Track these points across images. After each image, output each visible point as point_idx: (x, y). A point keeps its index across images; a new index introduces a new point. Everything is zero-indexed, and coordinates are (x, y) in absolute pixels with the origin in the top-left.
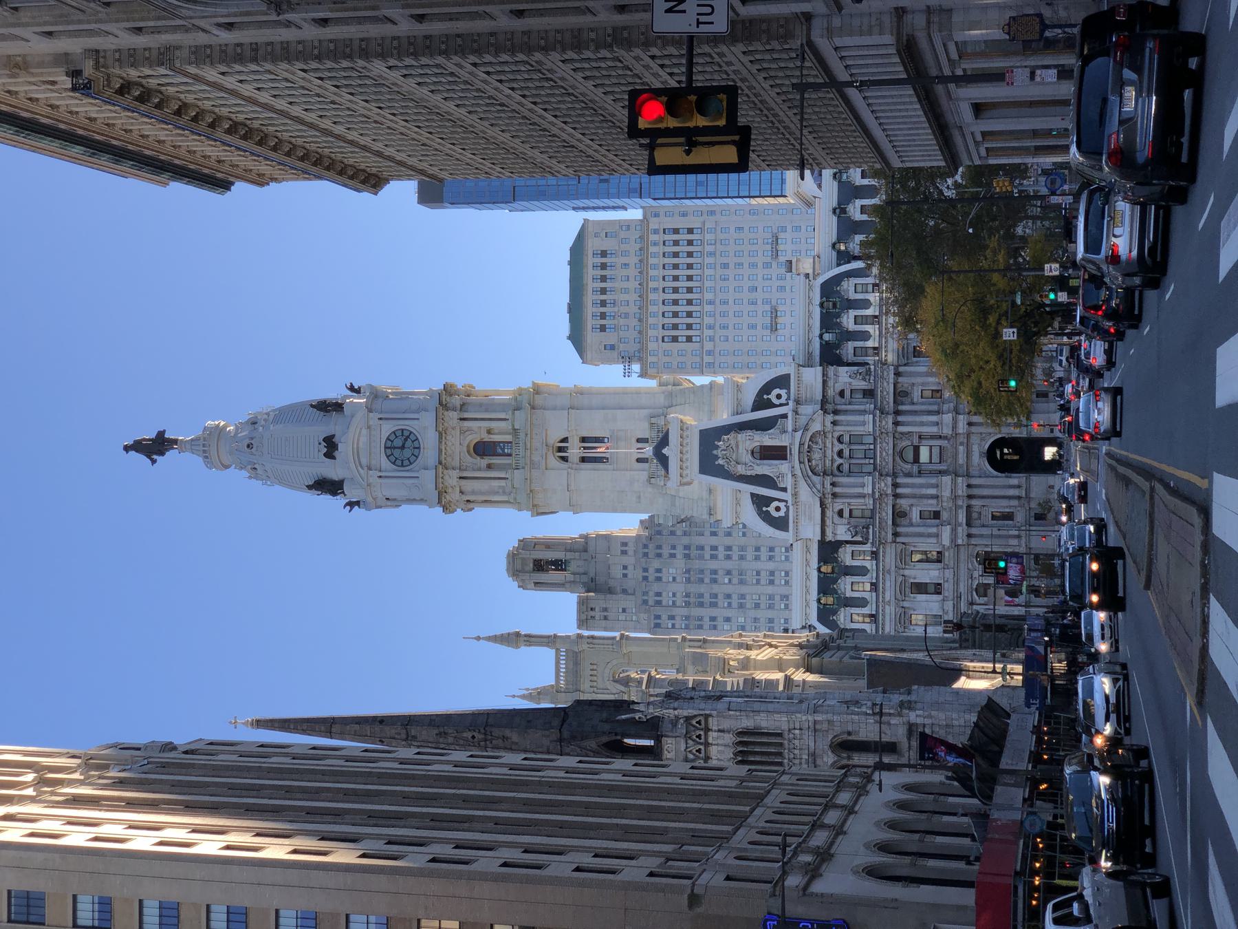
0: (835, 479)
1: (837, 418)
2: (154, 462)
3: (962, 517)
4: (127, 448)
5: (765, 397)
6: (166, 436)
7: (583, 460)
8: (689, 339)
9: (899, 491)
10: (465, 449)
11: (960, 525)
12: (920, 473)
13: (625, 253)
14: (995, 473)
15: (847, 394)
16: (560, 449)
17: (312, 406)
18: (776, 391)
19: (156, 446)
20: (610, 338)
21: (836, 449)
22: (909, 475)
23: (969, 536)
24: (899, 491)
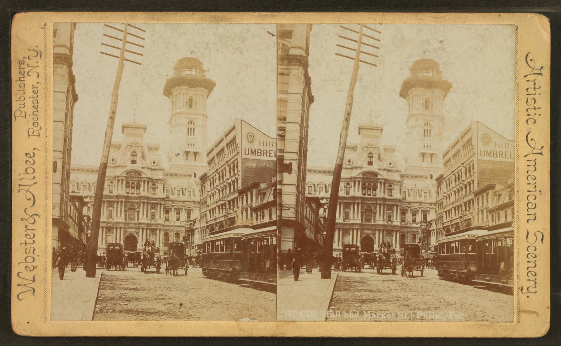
0: (124, 181)
1: (146, 182)
3: (109, 225)
9: (120, 204)
11: (107, 224)
12: (125, 211)
14: (125, 237)
21: (135, 182)
22: (125, 207)
23: (103, 228)
24: (120, 204)
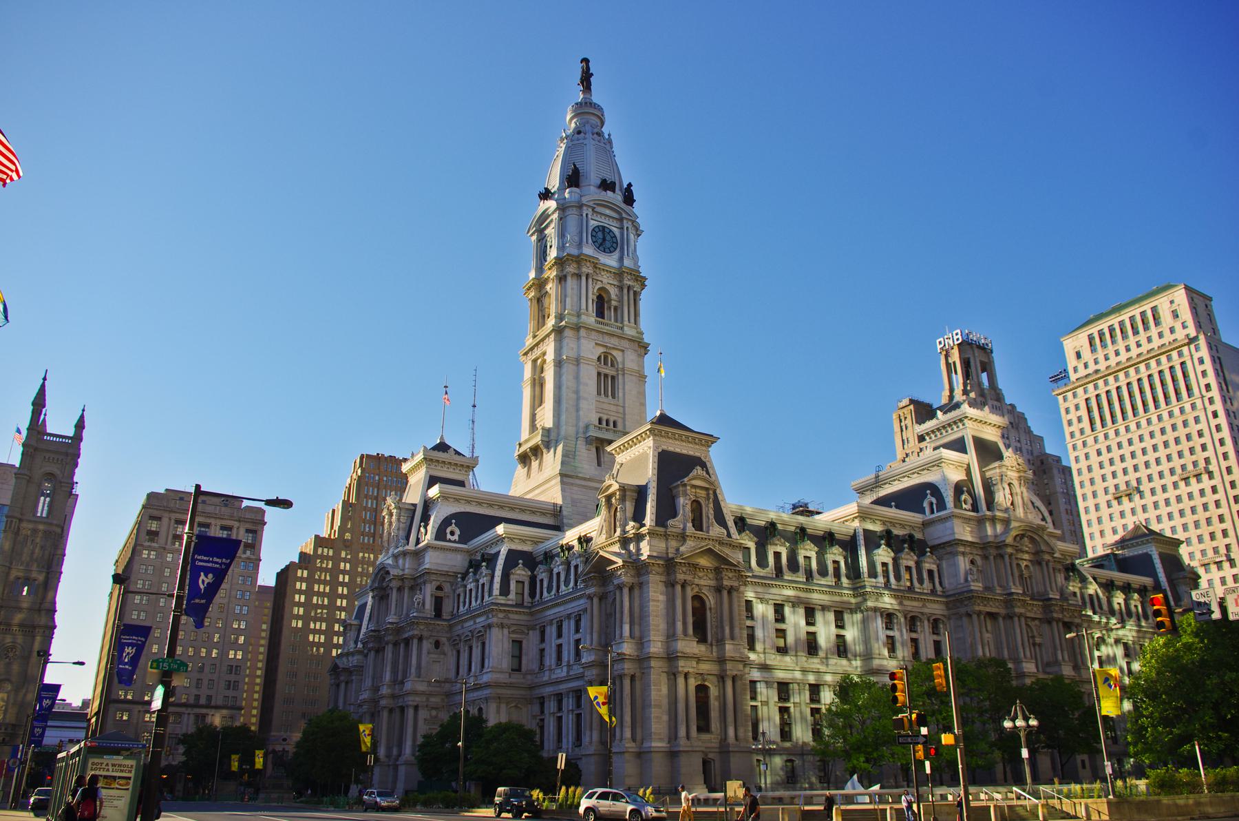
4: (586, 61)
13: (1160, 335)
19: (586, 80)
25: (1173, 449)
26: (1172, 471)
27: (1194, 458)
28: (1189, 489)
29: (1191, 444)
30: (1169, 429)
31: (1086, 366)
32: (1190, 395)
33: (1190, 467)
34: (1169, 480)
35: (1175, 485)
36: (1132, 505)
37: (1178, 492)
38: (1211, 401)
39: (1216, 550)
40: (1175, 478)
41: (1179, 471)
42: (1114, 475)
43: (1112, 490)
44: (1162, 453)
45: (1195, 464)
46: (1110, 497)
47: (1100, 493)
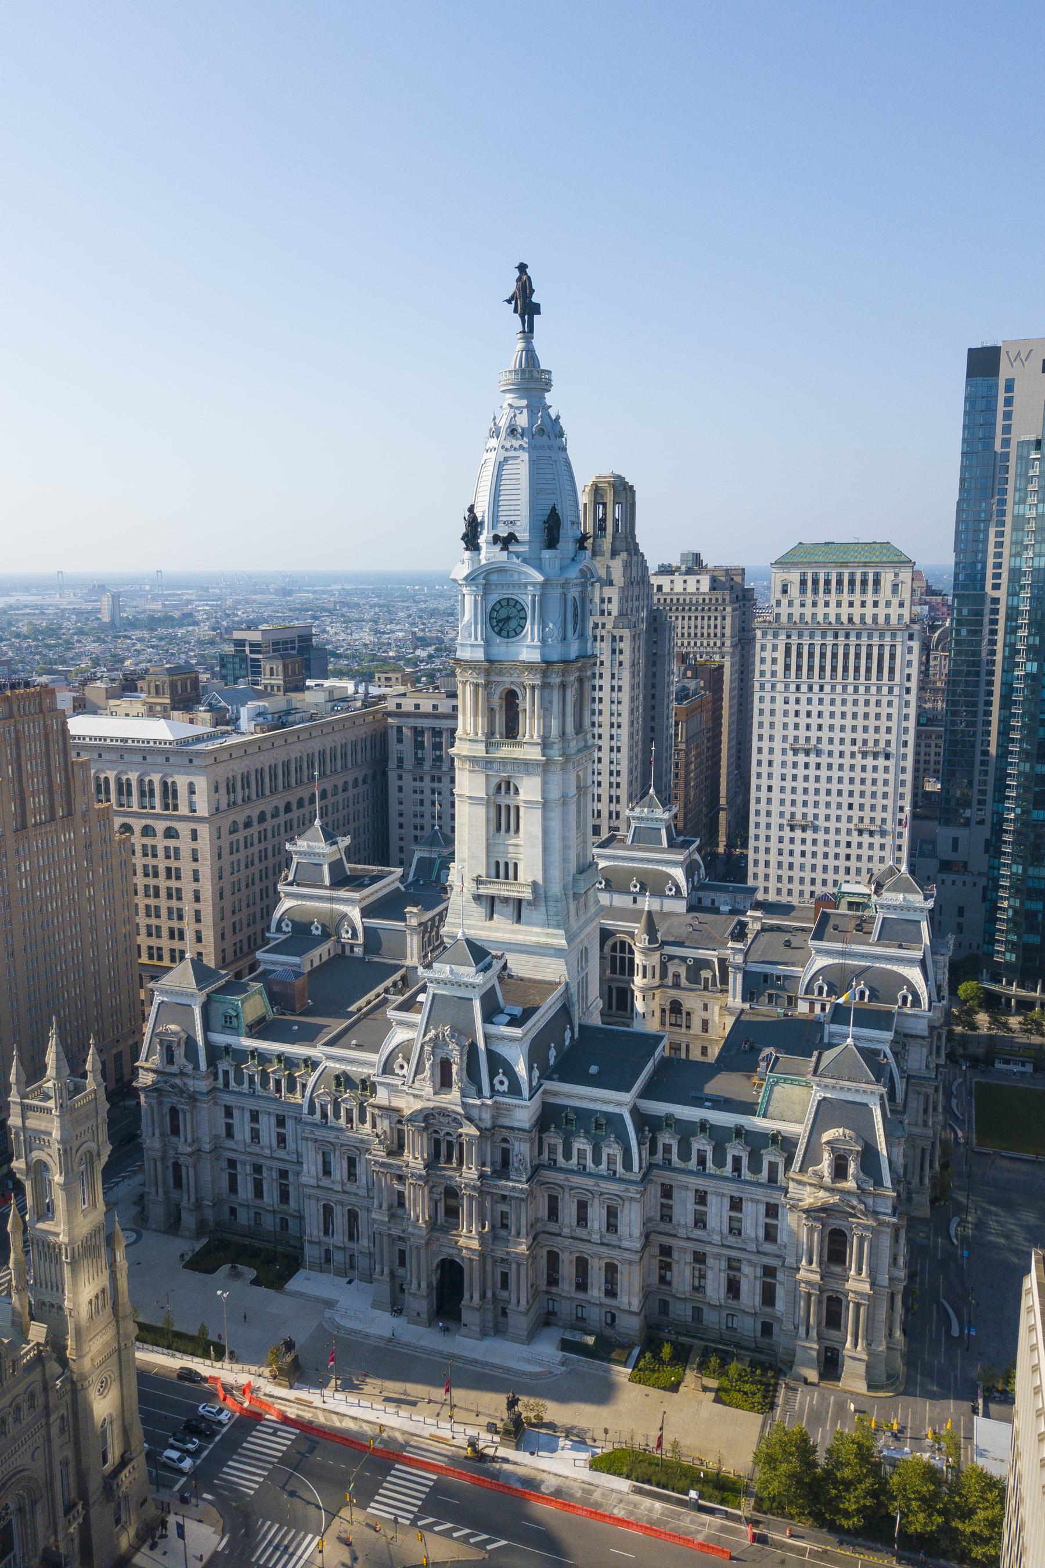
2: (509, 301)
4: (522, 268)
5: (501, 1071)
6: (536, 316)
7: (499, 807)
8: (787, 667)
10: (508, 686)
15: (505, 1145)
16: (508, 783)
17: (554, 509)
18: (506, 1083)
20: (794, 591)
25: (860, 722)
26: (854, 742)
27: (877, 736)
28: (864, 762)
29: (878, 723)
30: (861, 702)
31: (790, 604)
32: (891, 678)
33: (871, 743)
34: (848, 748)
35: (853, 755)
36: (807, 759)
37: (853, 761)
38: (908, 691)
39: (872, 820)
40: (855, 749)
41: (859, 743)
42: (797, 726)
43: (791, 740)
44: (849, 722)
45: (876, 742)
46: (787, 746)
47: (778, 738)
